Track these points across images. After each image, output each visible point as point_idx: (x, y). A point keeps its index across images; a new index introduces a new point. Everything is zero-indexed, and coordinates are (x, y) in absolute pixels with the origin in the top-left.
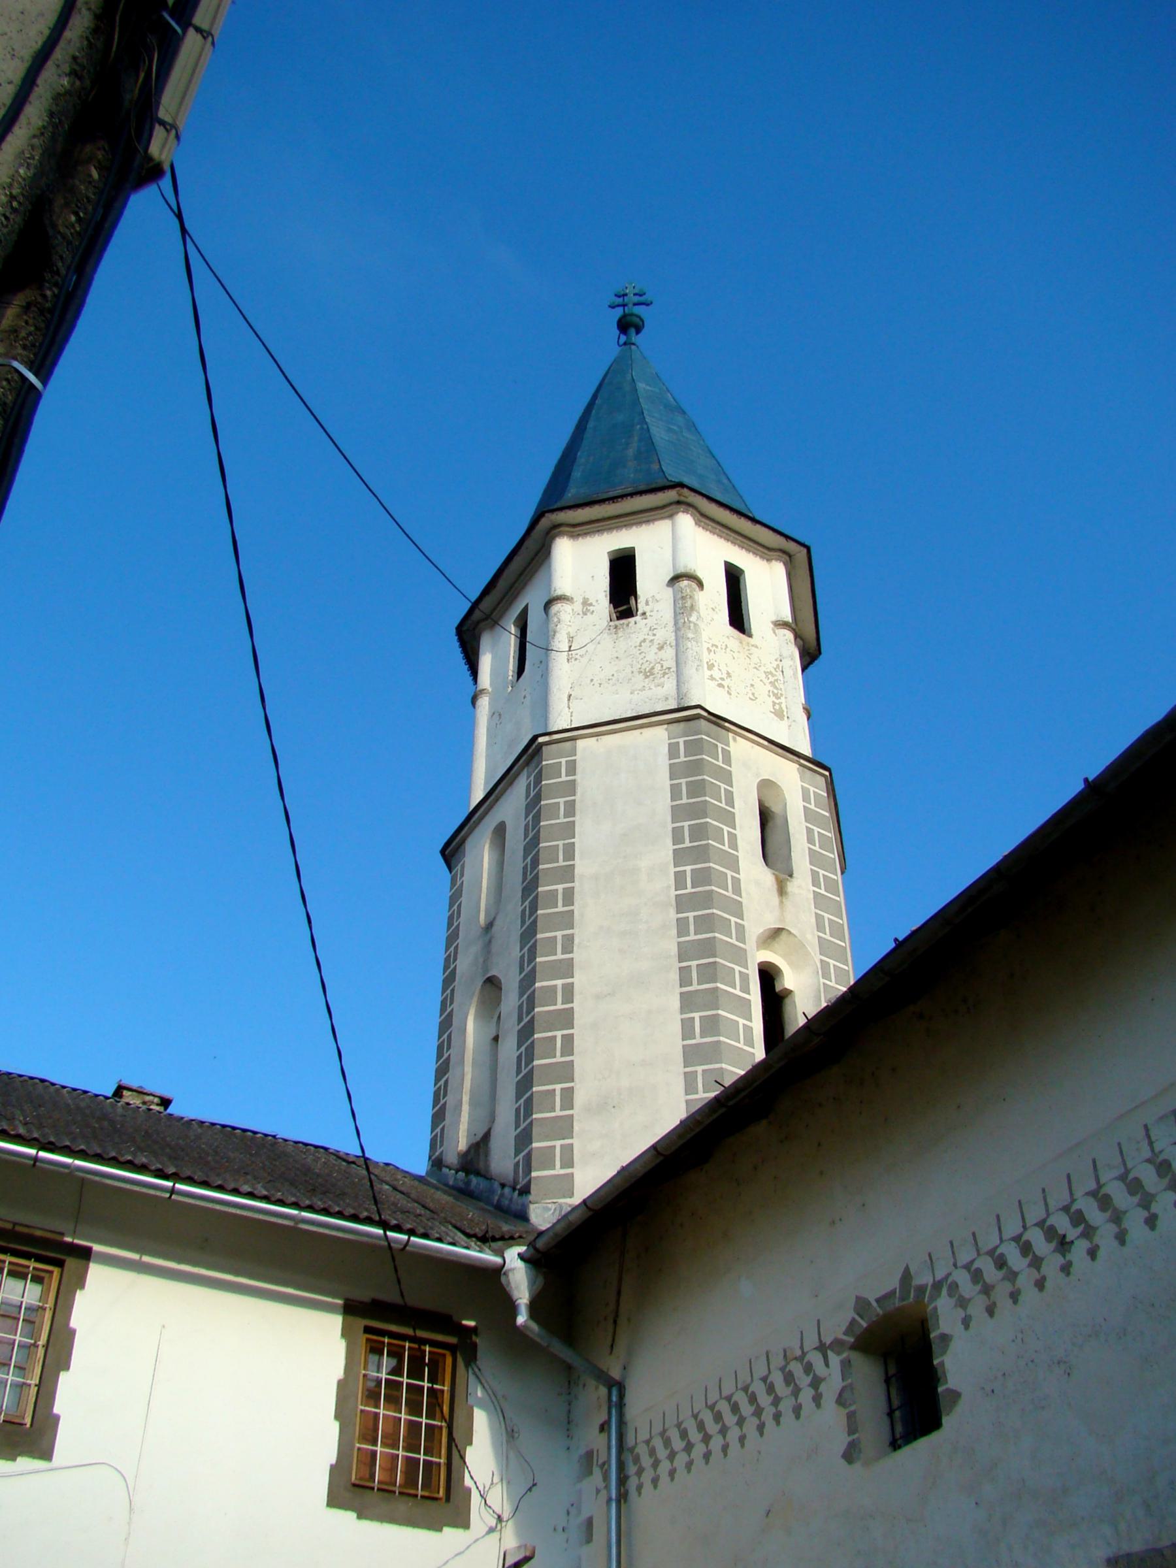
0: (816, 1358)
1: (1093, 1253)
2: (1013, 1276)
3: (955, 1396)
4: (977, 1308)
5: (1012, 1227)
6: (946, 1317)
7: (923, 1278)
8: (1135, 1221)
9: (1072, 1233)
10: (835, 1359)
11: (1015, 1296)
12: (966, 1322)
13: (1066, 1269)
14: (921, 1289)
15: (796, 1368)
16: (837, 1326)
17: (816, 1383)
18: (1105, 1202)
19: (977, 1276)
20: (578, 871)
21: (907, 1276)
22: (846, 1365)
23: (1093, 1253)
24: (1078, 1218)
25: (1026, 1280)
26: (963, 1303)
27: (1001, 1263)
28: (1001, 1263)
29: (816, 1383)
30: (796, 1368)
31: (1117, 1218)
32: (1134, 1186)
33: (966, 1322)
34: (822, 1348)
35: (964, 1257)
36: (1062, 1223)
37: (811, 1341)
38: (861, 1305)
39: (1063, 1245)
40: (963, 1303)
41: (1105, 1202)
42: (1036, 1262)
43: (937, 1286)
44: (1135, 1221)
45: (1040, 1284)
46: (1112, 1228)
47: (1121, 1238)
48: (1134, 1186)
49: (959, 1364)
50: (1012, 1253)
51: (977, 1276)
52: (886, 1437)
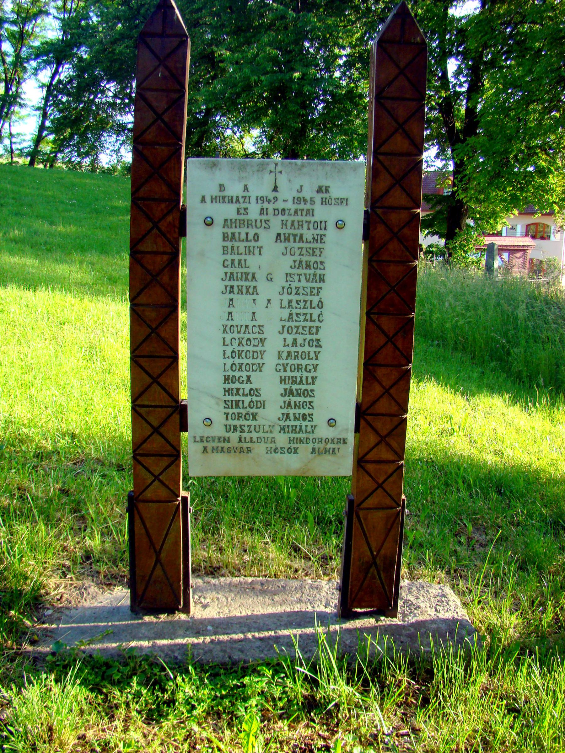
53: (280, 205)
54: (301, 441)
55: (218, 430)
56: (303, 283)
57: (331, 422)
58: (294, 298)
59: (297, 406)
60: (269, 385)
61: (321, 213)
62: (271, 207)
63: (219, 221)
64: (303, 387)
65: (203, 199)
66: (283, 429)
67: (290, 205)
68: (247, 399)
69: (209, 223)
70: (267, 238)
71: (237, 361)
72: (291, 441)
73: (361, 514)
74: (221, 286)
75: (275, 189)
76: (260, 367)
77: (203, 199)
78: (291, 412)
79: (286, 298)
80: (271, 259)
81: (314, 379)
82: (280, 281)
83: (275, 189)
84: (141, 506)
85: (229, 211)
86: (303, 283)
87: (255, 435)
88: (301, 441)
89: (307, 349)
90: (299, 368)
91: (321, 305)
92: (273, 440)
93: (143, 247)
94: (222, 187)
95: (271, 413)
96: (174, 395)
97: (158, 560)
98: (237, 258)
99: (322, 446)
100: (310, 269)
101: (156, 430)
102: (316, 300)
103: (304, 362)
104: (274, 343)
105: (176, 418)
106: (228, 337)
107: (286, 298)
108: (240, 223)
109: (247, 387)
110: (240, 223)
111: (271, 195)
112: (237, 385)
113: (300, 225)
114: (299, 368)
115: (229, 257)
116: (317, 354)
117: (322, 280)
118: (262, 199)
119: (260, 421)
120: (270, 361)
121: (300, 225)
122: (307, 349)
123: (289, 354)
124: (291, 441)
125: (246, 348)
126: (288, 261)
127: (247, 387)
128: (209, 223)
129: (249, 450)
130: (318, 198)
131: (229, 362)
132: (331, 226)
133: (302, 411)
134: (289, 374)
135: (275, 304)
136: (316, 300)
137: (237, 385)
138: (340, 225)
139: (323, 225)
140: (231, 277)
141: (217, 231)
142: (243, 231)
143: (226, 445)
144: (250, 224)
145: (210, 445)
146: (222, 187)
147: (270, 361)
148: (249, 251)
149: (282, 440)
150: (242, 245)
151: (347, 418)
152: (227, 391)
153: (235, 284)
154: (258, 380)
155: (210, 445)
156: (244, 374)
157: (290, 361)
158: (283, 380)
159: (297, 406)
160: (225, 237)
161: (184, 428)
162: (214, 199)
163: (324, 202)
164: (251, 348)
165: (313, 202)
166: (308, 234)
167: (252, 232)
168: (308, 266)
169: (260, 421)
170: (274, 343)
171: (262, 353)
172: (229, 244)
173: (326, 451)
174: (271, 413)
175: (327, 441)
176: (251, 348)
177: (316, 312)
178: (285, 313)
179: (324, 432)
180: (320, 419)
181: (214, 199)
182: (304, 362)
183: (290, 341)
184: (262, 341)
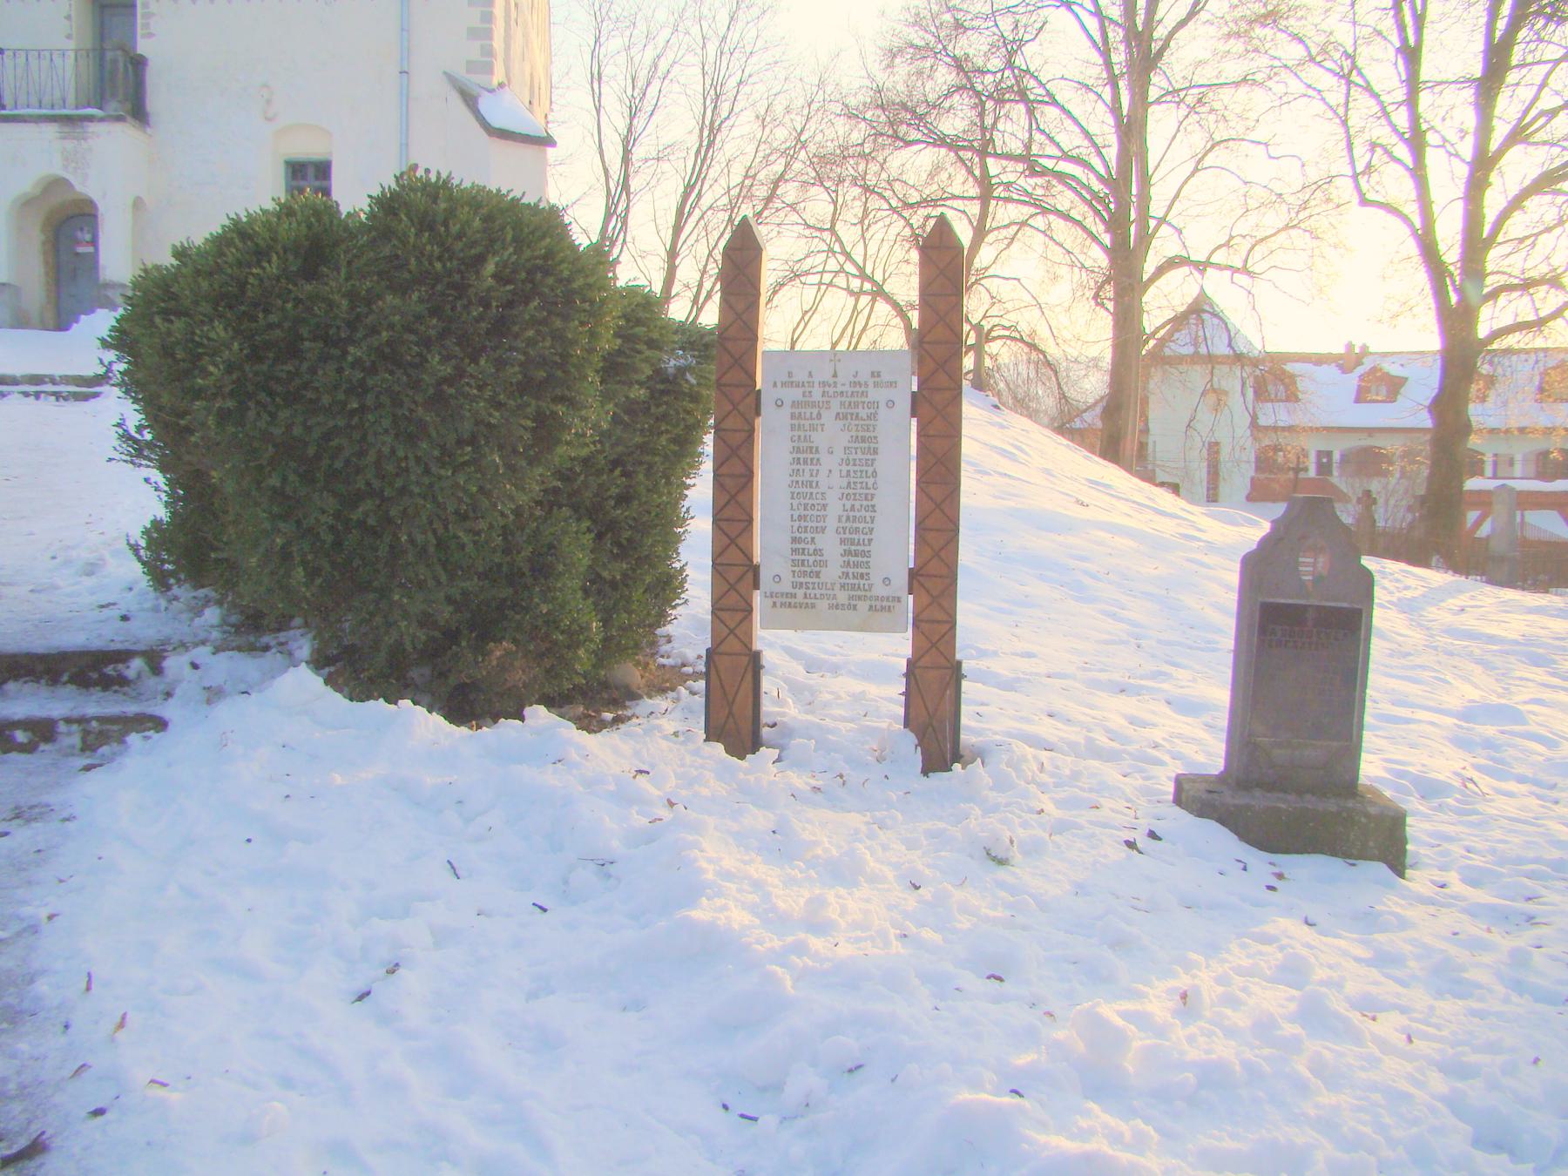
53: (840, 388)
54: (860, 598)
55: (786, 587)
56: (860, 456)
57: (887, 581)
58: (851, 468)
59: (856, 565)
60: (830, 545)
61: (875, 394)
62: (831, 390)
63: (788, 402)
64: (860, 548)
65: (775, 385)
66: (843, 586)
67: (847, 388)
68: (812, 559)
69: (779, 404)
70: (828, 417)
71: (803, 524)
72: (851, 598)
73: (917, 672)
74: (789, 458)
75: (835, 376)
76: (823, 530)
77: (775, 385)
78: (851, 571)
79: (845, 468)
80: (832, 436)
81: (870, 541)
82: (839, 454)
83: (835, 376)
84: (716, 658)
85: (795, 394)
86: (860, 456)
87: (818, 592)
88: (860, 598)
89: (863, 513)
90: (857, 530)
91: (875, 474)
92: (835, 597)
93: (723, 426)
94: (790, 374)
95: (832, 572)
96: (750, 560)
97: (730, 713)
98: (802, 434)
99: (878, 603)
100: (866, 444)
101: (732, 587)
102: (870, 470)
103: (861, 526)
104: (835, 508)
105: (750, 575)
106: (795, 502)
107: (845, 468)
108: (807, 404)
109: (812, 548)
110: (807, 404)
111: (831, 381)
112: (802, 546)
113: (856, 405)
114: (857, 530)
115: (796, 433)
116: (873, 519)
117: (875, 452)
118: (824, 384)
119: (823, 579)
120: (831, 523)
121: (856, 405)
122: (863, 513)
123: (848, 518)
124: (851, 598)
125: (810, 512)
126: (846, 436)
127: (812, 548)
128: (779, 404)
129: (813, 606)
130: (871, 382)
131: (796, 524)
132: (882, 406)
133: (860, 570)
134: (848, 535)
135: (836, 474)
136: (870, 470)
137: (802, 546)
138: (891, 404)
139: (875, 404)
140: (798, 450)
141: (787, 410)
142: (808, 411)
143: (793, 601)
144: (813, 405)
145: (779, 600)
146: (790, 374)
147: (831, 523)
148: (813, 428)
149: (842, 597)
150: (807, 423)
151: (902, 580)
152: (794, 551)
153: (801, 456)
154: (822, 541)
155: (779, 600)
156: (809, 536)
157: (848, 525)
158: (842, 541)
159: (856, 565)
160: (793, 416)
161: (756, 586)
162: (784, 384)
163: (876, 385)
164: (815, 513)
165: (866, 385)
166: (863, 413)
167: (815, 411)
168: (863, 440)
169: (823, 579)
170: (835, 508)
171: (825, 517)
172: (796, 422)
173: (883, 608)
174: (832, 572)
175: (882, 599)
176: (815, 513)
177: (871, 481)
178: (844, 482)
179: (879, 590)
180: (876, 579)
181: (784, 384)
182: (861, 526)
183: (848, 507)
184: (825, 506)
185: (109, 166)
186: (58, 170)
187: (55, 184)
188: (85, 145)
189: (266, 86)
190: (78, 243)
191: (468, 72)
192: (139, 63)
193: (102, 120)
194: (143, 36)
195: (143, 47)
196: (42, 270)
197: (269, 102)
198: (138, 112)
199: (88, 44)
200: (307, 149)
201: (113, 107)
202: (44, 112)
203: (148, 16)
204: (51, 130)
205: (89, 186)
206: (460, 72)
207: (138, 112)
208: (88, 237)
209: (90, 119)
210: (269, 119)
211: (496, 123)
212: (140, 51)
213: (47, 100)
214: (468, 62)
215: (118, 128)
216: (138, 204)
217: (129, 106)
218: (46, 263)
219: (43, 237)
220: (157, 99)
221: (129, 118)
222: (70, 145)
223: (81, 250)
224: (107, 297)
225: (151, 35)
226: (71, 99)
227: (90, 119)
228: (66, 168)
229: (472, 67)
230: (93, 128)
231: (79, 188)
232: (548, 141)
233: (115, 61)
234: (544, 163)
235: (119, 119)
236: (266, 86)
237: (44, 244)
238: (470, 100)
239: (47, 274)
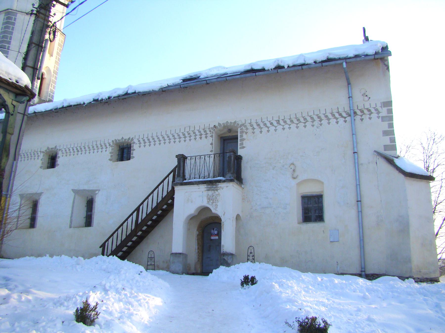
0: (39, 153)
1: (81, 154)
2: (70, 152)
3: (58, 165)
4: (65, 155)
5: (72, 146)
6: (60, 154)
7: (58, 148)
8: (88, 152)
9: (80, 150)
10: (42, 154)
11: (70, 155)
12: (63, 156)
13: (78, 154)
14: (57, 149)
15: (36, 153)
16: (44, 149)
17: (38, 156)
18: (85, 148)
19: (66, 150)
20: (12, 43)
21: (56, 147)
22: (44, 155)
23: (81, 154)
24: (81, 149)
25: (72, 153)
26: (63, 153)
27: (69, 150)
28: (69, 150)
29: (38, 156)
30: (36, 153)
31: (86, 151)
32: (89, 148)
33: (63, 156)
34: (41, 152)
35: (65, 147)
36: (79, 148)
37: (39, 150)
38: (48, 148)
39: (78, 151)
40: (63, 153)
41: (85, 148)
42: (74, 152)
43: (60, 150)
44: (88, 152)
45: (74, 155)
46: (85, 152)
47: (85, 153)
48: (89, 148)
49: (60, 161)
50: (71, 149)
51: (66, 150)
52: (47, 166)
185: (227, 201)
186: (205, 203)
187: (205, 210)
188: (217, 193)
189: (293, 164)
190: (212, 235)
191: (385, 150)
192: (239, 158)
193: (224, 181)
194: (240, 148)
195: (240, 152)
196: (197, 247)
197: (294, 171)
198: (238, 178)
199: (219, 151)
200: (311, 189)
201: (228, 176)
202: (201, 180)
203: (243, 140)
204: (203, 187)
205: (218, 210)
206: (382, 151)
207: (238, 178)
208: (216, 232)
209: (220, 181)
210: (294, 178)
211: (408, 170)
212: (239, 153)
213: (202, 175)
214: (384, 146)
215: (231, 184)
216: (238, 217)
217: (235, 175)
218: (198, 244)
219: (198, 233)
220: (246, 173)
221: (235, 180)
222: (210, 193)
223: (213, 238)
224: (224, 259)
225: (243, 147)
226: (211, 175)
227: (220, 181)
228: (208, 202)
229: (386, 147)
230: (220, 185)
231: (213, 211)
232: (431, 178)
233: (230, 157)
234: (429, 188)
235: (231, 181)
236: (293, 164)
237: (198, 235)
238: (390, 161)
239: (198, 248)
